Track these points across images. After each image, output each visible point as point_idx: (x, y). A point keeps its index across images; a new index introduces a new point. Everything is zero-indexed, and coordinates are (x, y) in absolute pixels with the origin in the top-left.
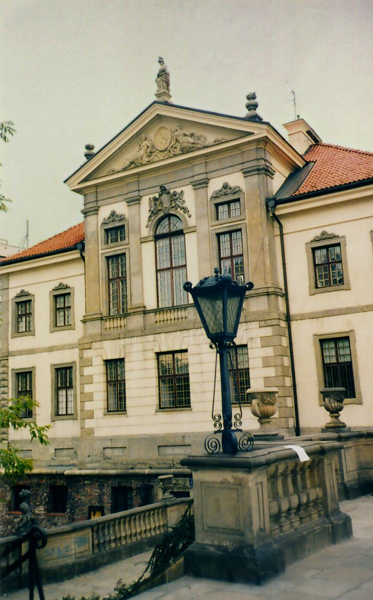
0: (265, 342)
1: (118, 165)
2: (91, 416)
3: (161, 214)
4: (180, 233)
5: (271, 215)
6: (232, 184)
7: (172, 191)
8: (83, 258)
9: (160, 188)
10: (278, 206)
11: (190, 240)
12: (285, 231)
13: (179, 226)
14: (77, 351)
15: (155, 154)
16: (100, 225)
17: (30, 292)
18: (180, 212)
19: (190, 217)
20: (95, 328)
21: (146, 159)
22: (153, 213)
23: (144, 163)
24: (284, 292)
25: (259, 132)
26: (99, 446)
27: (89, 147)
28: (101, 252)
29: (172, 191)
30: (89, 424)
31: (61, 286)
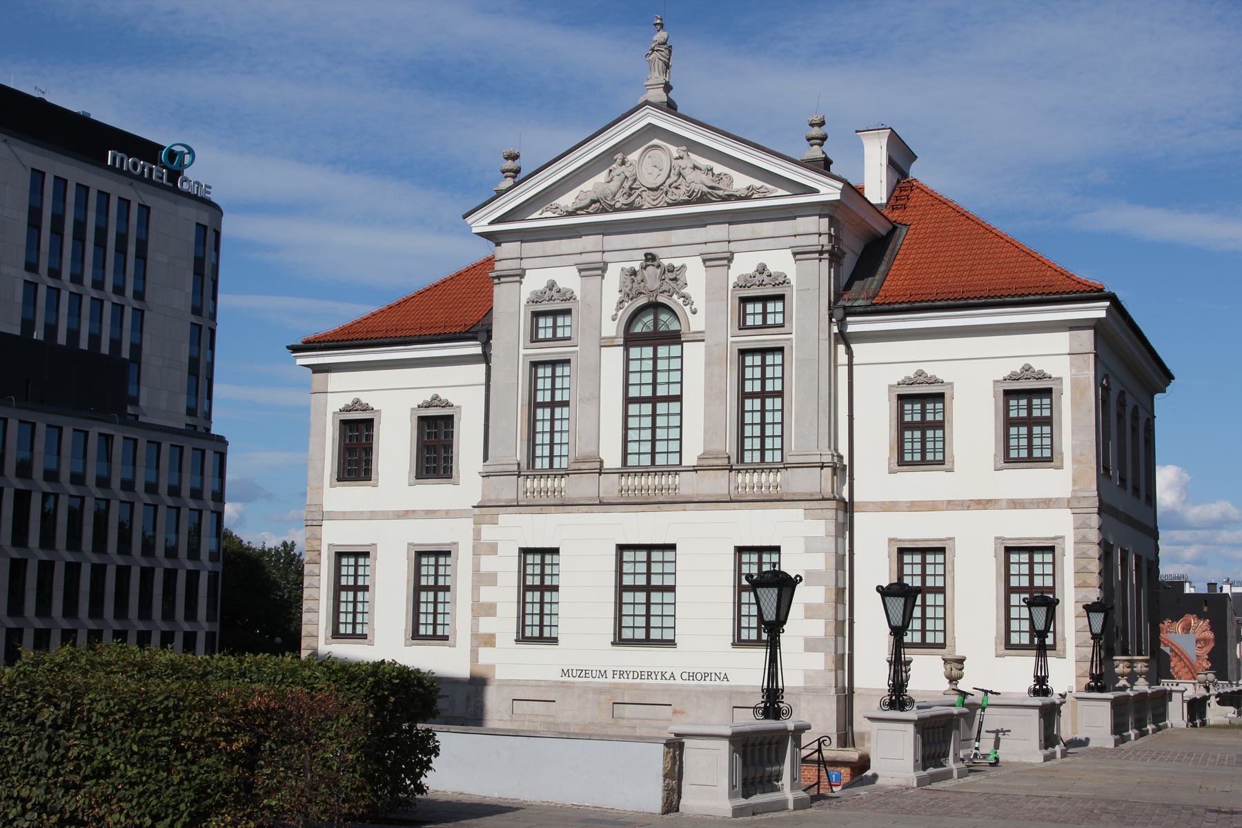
0: (810, 546)
1: (567, 200)
2: (489, 640)
3: (642, 301)
4: (674, 338)
5: (835, 329)
6: (772, 269)
7: (665, 262)
8: (486, 358)
9: (646, 255)
10: (848, 319)
11: (694, 354)
12: (855, 361)
13: (674, 326)
14: (469, 523)
15: (638, 192)
16: (524, 302)
17: (371, 405)
18: (675, 302)
19: (694, 312)
20: (507, 489)
21: (621, 201)
22: (629, 296)
23: (618, 205)
24: (846, 462)
25: (829, 191)
28: (522, 352)
30: (486, 656)
31: (435, 402)
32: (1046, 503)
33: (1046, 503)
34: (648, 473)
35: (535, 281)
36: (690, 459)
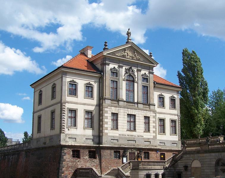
3: (129, 74)
7: (133, 69)
26: (110, 138)
27: (106, 43)
29: (133, 69)
32: (175, 115)
33: (175, 115)
34: (130, 102)
35: (112, 66)
36: (136, 101)
